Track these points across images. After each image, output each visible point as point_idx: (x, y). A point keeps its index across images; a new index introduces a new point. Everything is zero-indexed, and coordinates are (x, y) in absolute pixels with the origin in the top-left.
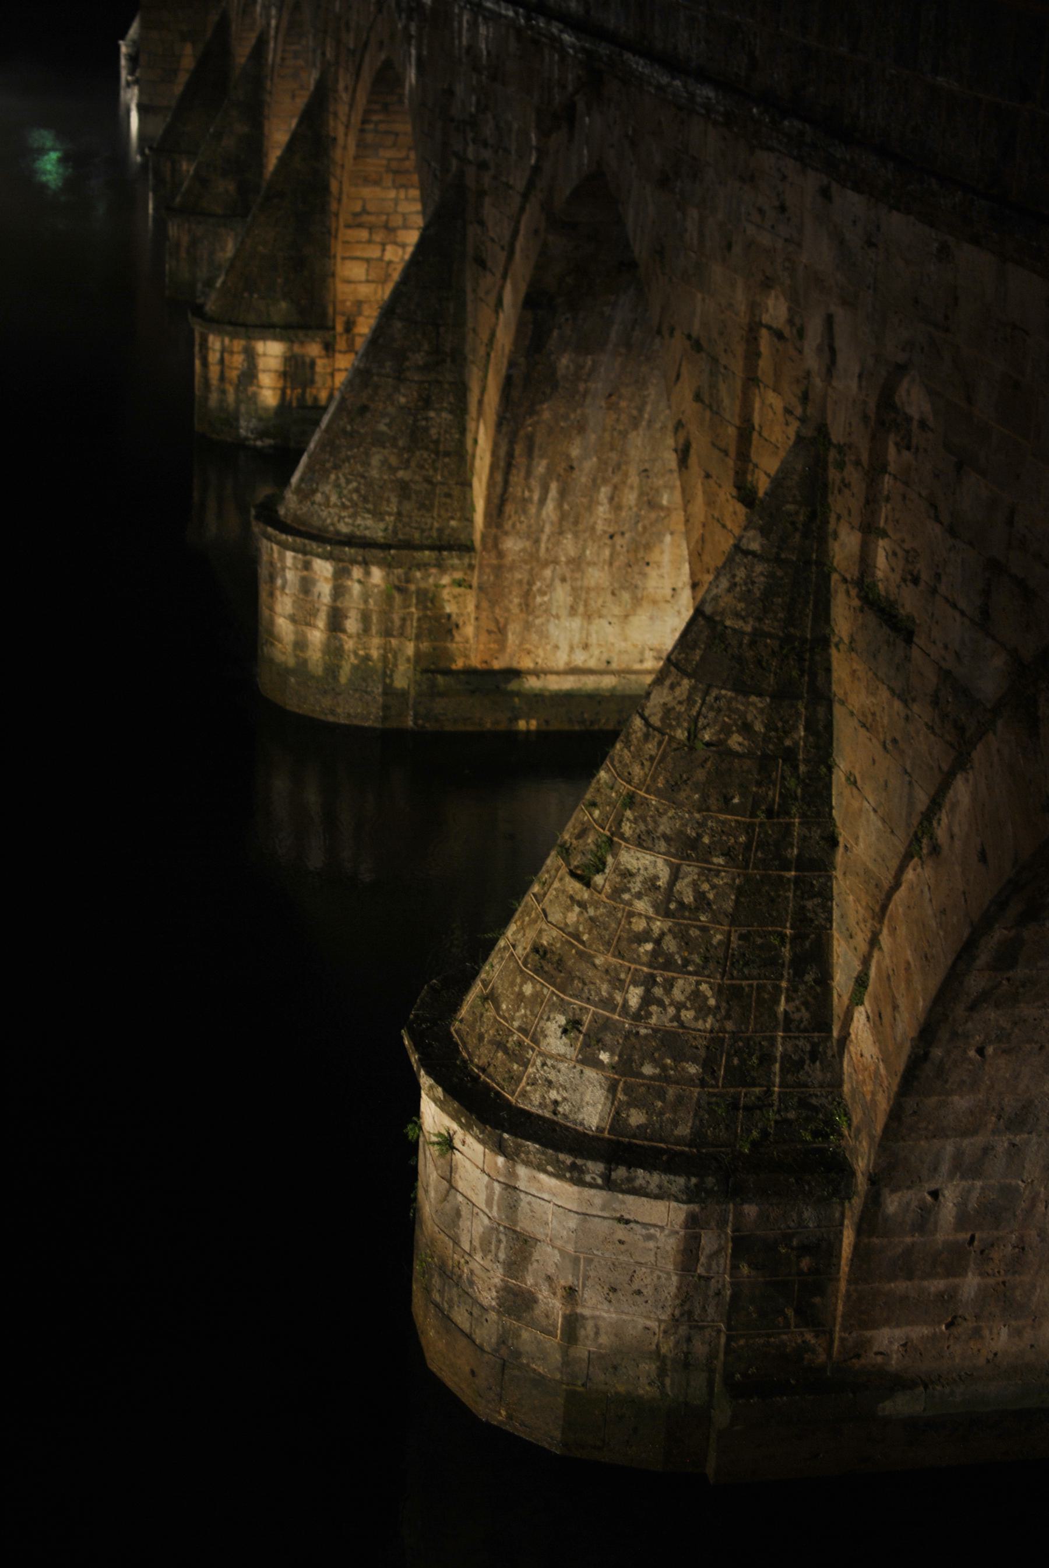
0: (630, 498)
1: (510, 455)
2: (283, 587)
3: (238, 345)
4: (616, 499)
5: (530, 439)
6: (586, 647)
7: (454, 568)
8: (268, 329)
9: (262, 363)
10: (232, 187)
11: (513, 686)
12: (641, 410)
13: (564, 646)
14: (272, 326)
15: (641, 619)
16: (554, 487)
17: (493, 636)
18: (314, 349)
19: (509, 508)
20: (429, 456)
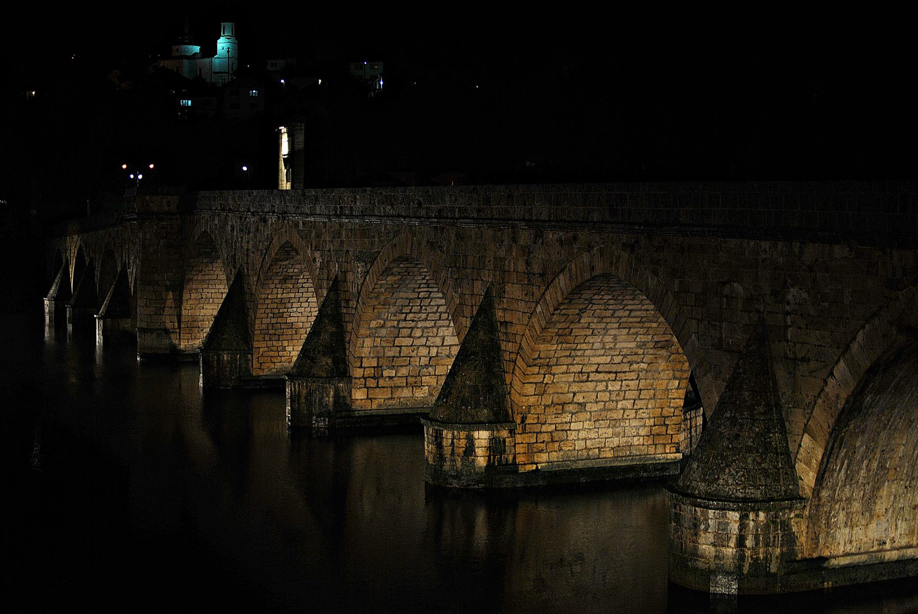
0: (875, 465)
1: (832, 448)
2: (706, 530)
3: (463, 434)
4: (869, 466)
5: (842, 440)
6: (851, 542)
7: (796, 509)
8: (480, 425)
9: (477, 443)
10: (330, 361)
11: (825, 565)
12: (889, 421)
13: (842, 543)
14: (481, 423)
15: (873, 526)
16: (846, 462)
17: (814, 541)
18: (505, 434)
19: (826, 475)
20: (774, 455)
